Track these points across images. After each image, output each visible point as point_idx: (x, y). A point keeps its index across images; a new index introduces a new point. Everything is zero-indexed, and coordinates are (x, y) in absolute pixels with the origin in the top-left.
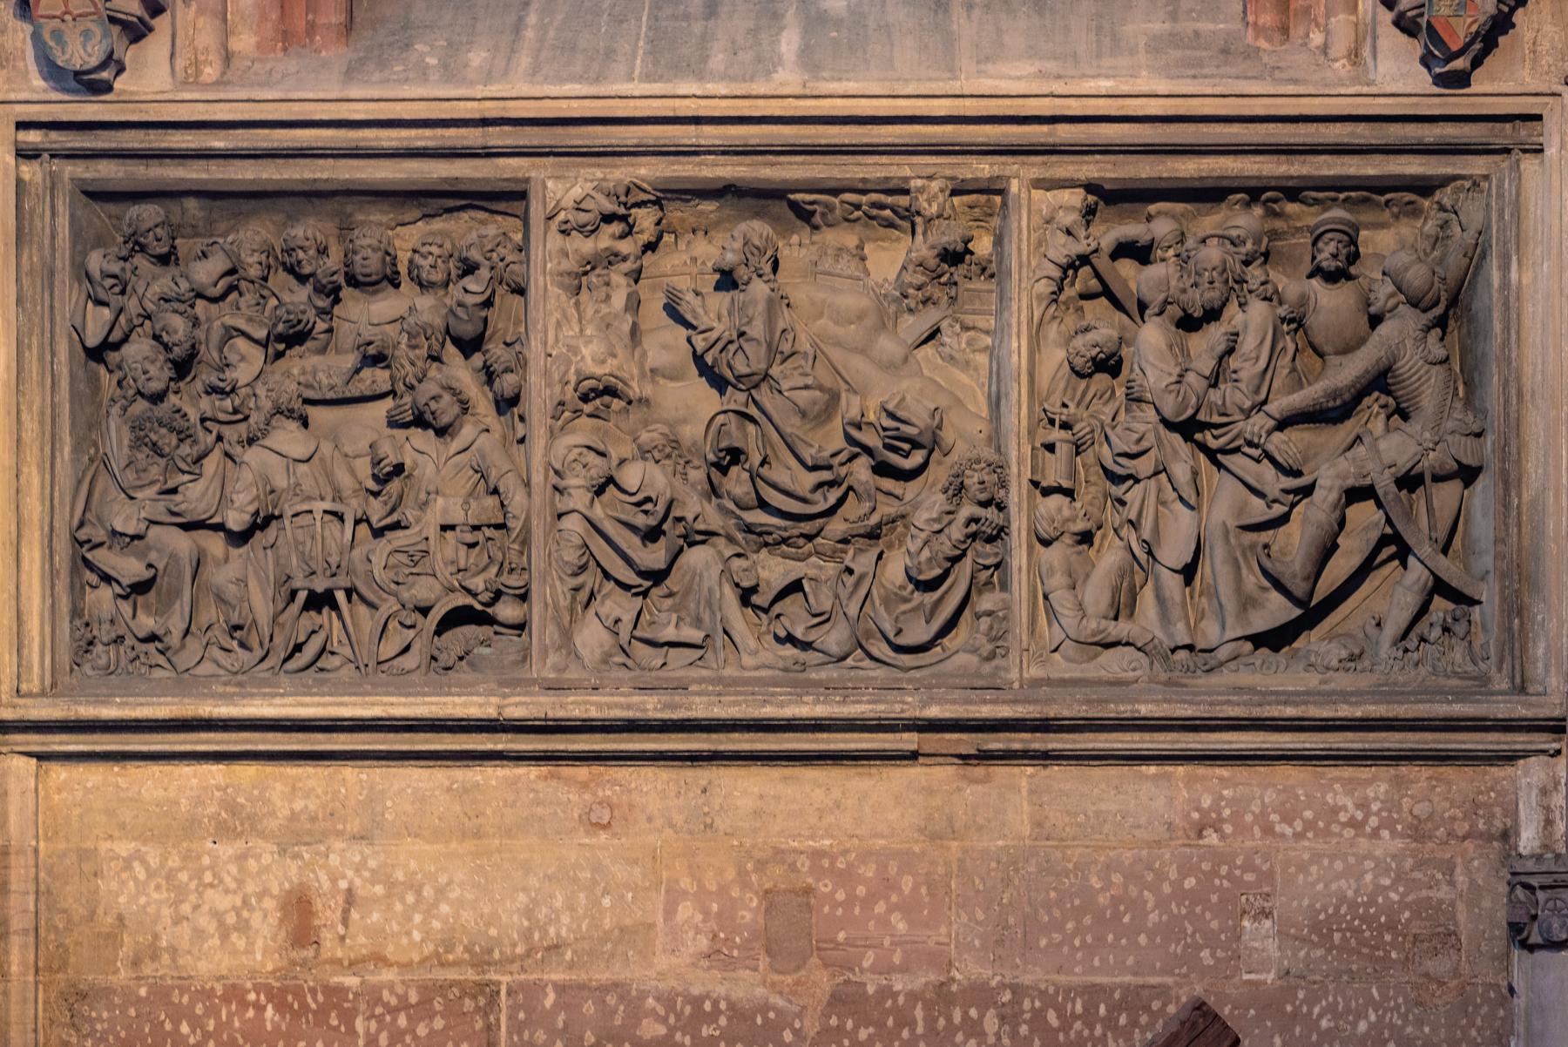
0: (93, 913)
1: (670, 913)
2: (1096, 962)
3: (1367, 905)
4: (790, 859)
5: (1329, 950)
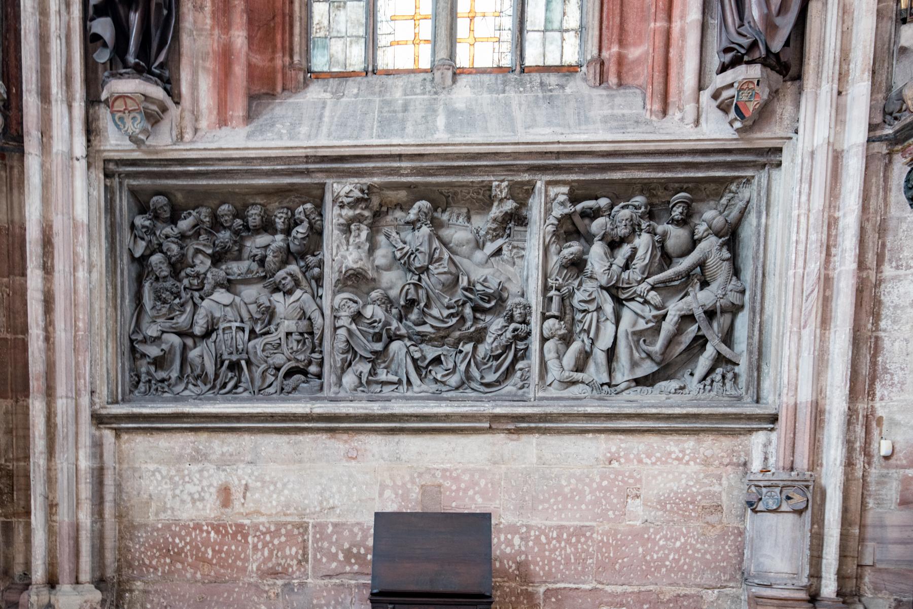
0: (139, 494)
1: (381, 494)
2: (563, 516)
3: (682, 493)
4: (433, 472)
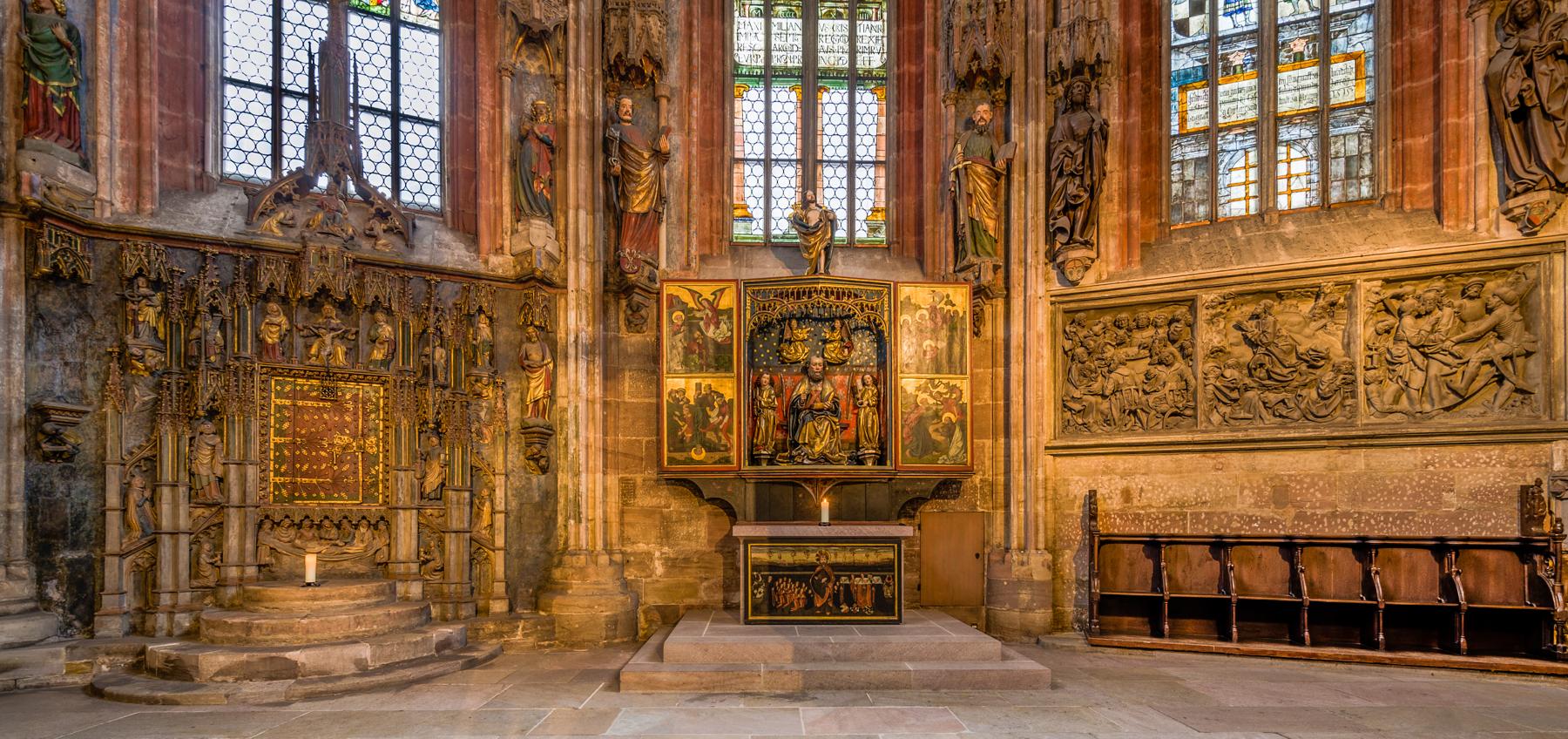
1: (1241, 493)
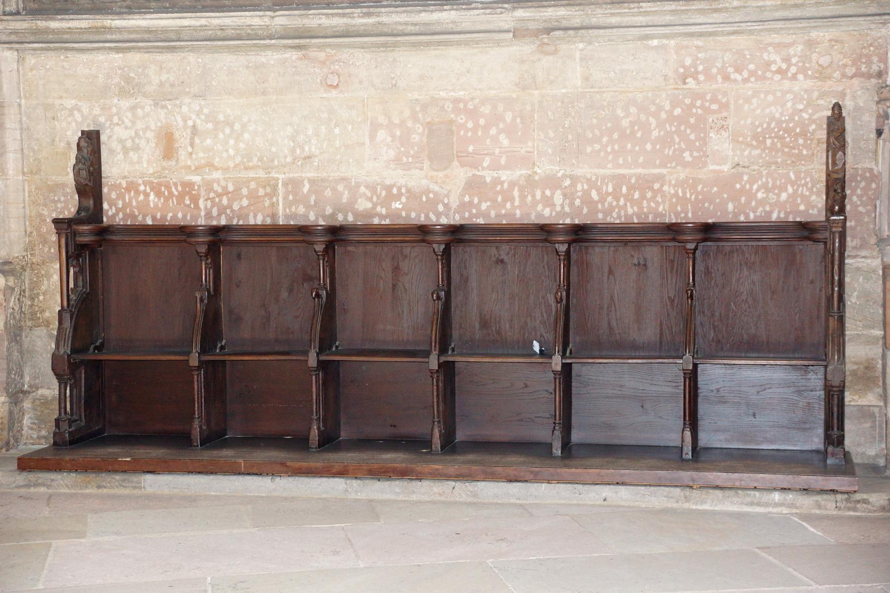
0: (53, 140)
1: (372, 137)
5: (763, 150)
